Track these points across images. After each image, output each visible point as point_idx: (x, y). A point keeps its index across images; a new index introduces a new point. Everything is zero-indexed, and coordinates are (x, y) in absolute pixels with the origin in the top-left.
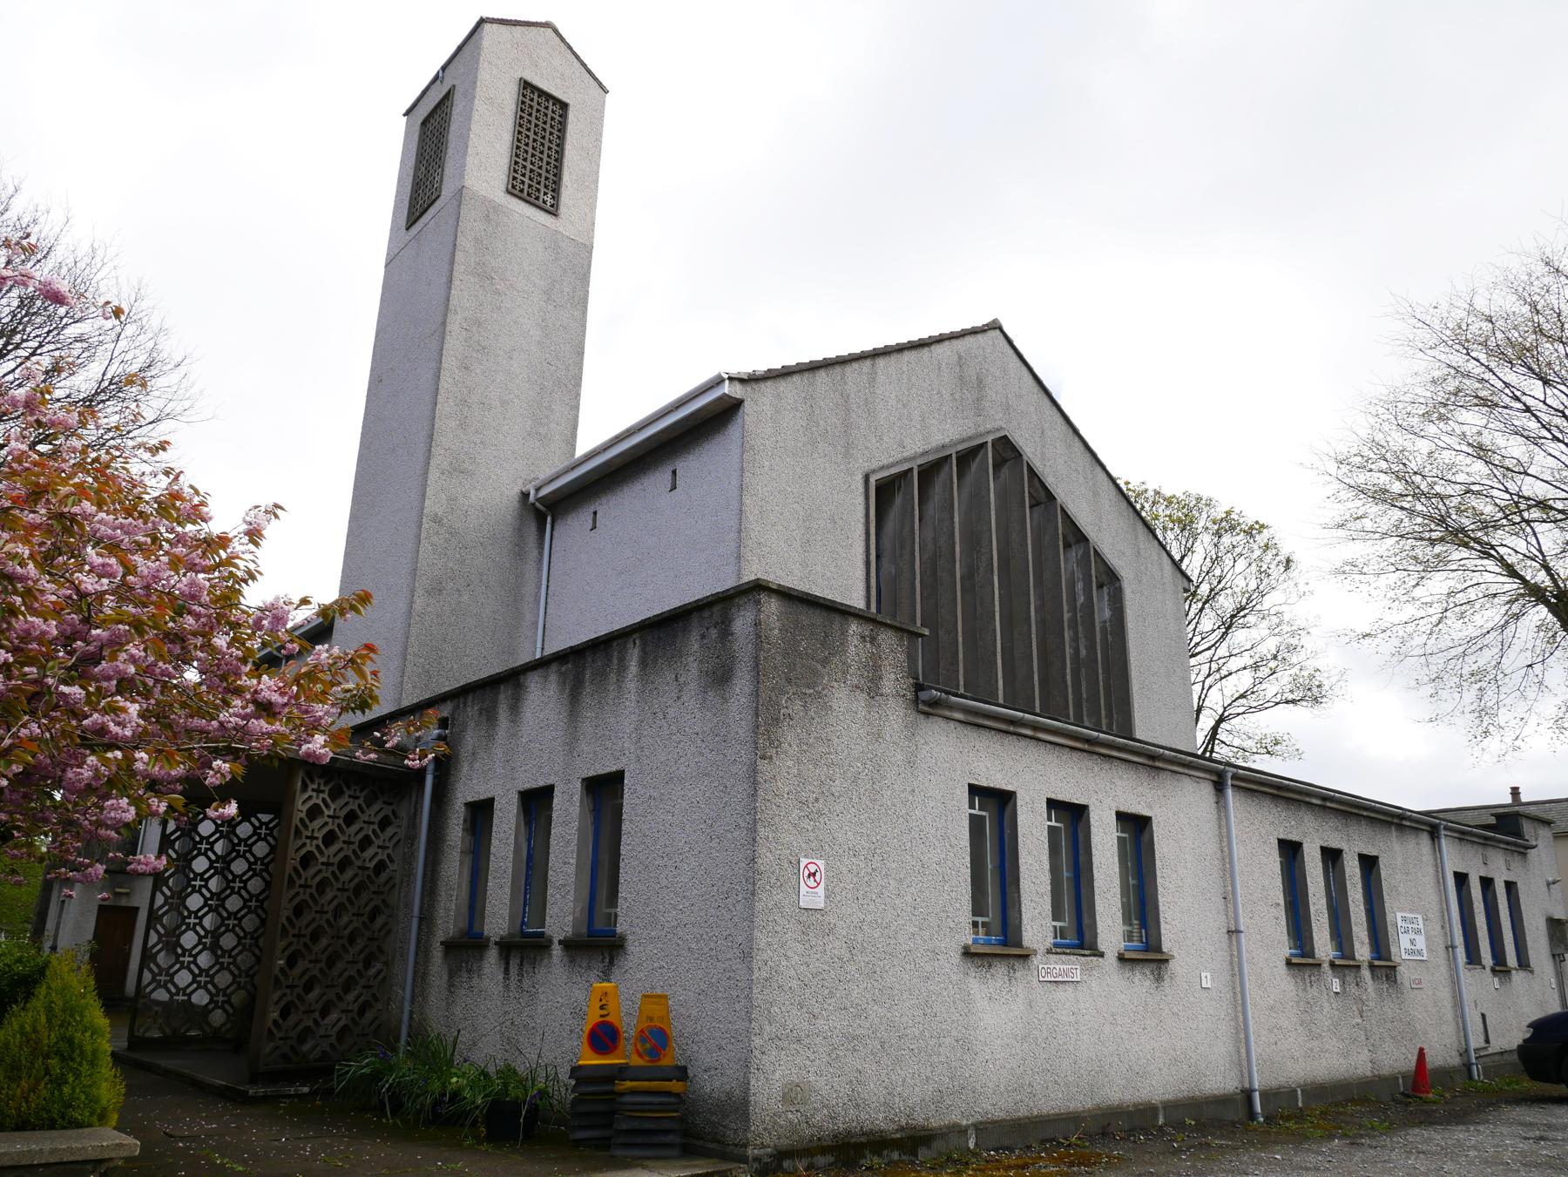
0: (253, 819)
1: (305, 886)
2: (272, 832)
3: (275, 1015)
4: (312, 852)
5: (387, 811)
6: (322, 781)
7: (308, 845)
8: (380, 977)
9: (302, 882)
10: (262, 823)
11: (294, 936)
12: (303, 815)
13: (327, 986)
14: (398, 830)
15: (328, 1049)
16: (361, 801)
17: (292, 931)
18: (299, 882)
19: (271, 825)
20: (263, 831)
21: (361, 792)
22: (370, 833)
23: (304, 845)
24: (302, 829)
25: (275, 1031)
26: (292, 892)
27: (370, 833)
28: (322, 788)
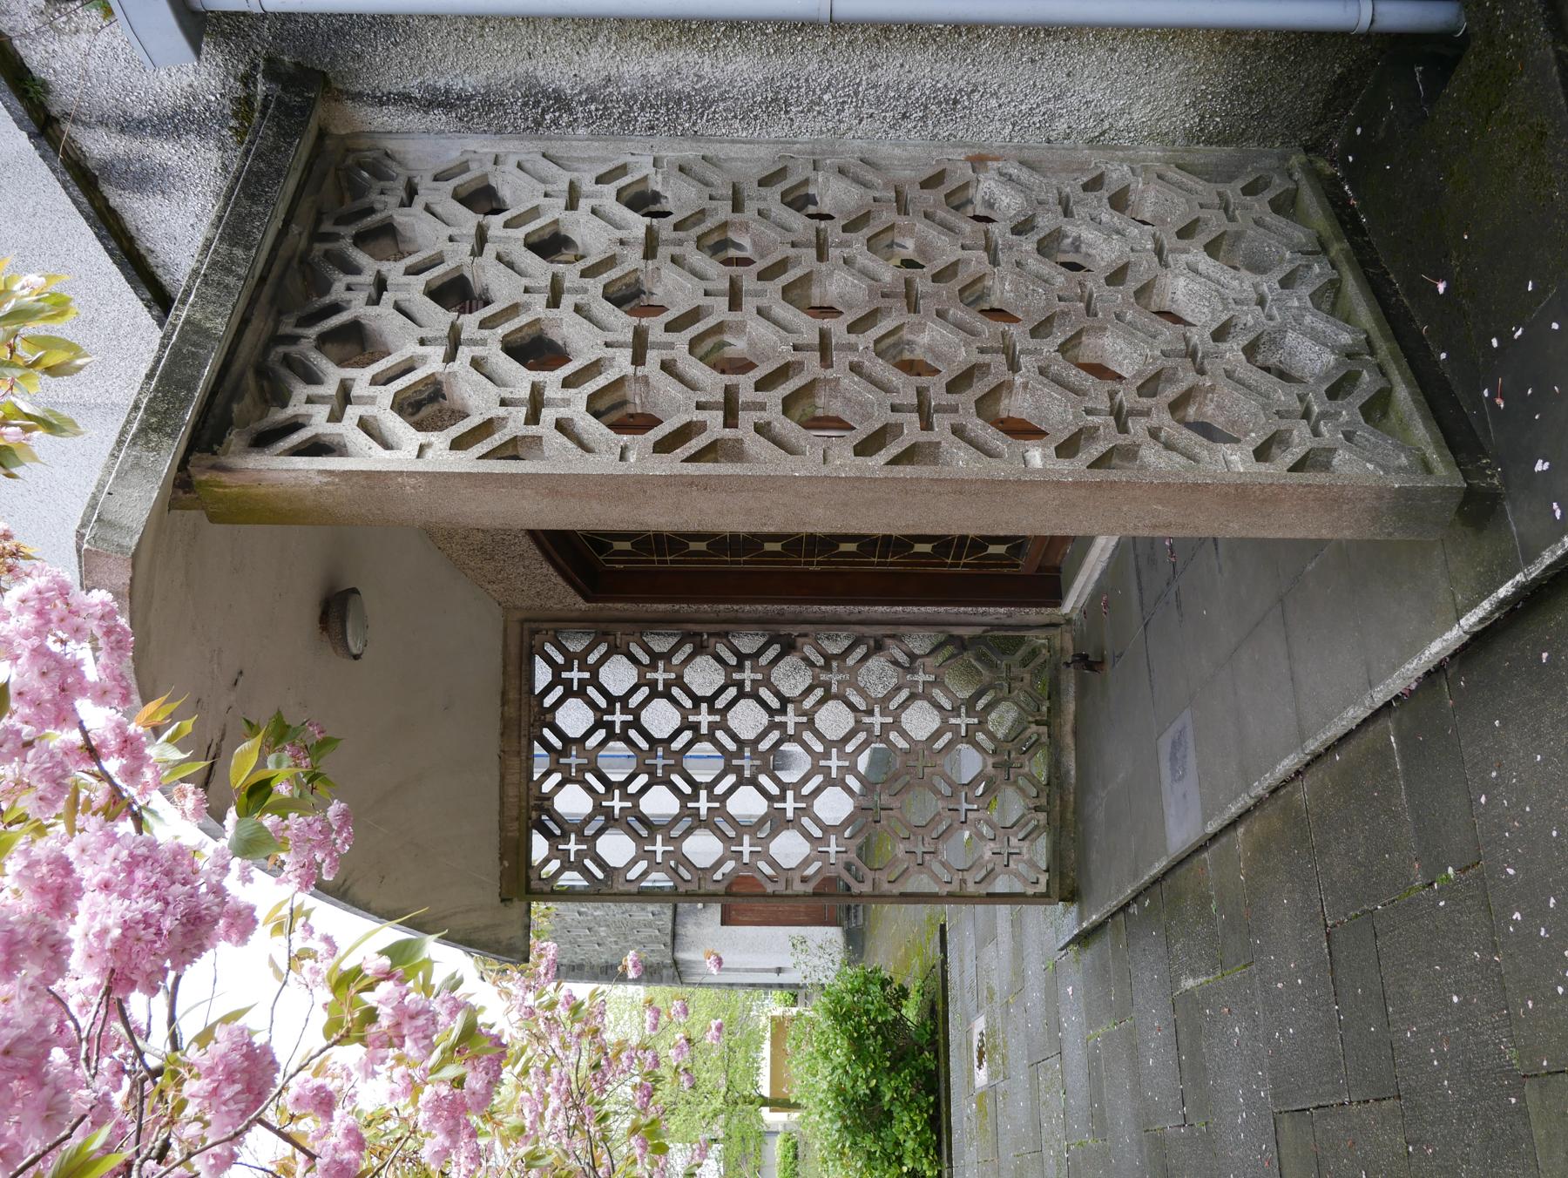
0: (547, 787)
1: (730, 409)
2: (661, 656)
3: (1036, 456)
4: (592, 398)
5: (442, 196)
6: (301, 391)
7: (563, 412)
8: (1024, 175)
9: (715, 418)
10: (556, 681)
11: (927, 425)
12: (439, 441)
13: (1090, 311)
14: (512, 162)
15: (1305, 291)
16: (361, 378)
17: (912, 431)
18: (912, 431)
19: (560, 659)
20: (575, 675)
21: (357, 271)
22: (520, 233)
23: (562, 426)
24: (497, 439)
25: (1096, 450)
26: (756, 445)
27: (520, 233)
28: (330, 388)
